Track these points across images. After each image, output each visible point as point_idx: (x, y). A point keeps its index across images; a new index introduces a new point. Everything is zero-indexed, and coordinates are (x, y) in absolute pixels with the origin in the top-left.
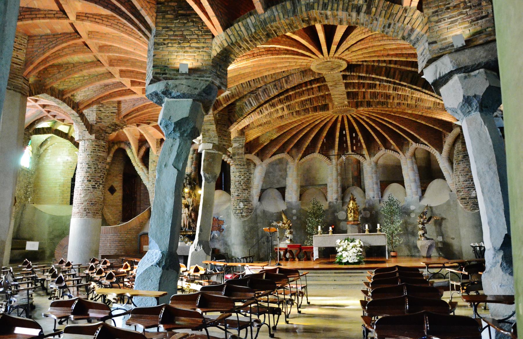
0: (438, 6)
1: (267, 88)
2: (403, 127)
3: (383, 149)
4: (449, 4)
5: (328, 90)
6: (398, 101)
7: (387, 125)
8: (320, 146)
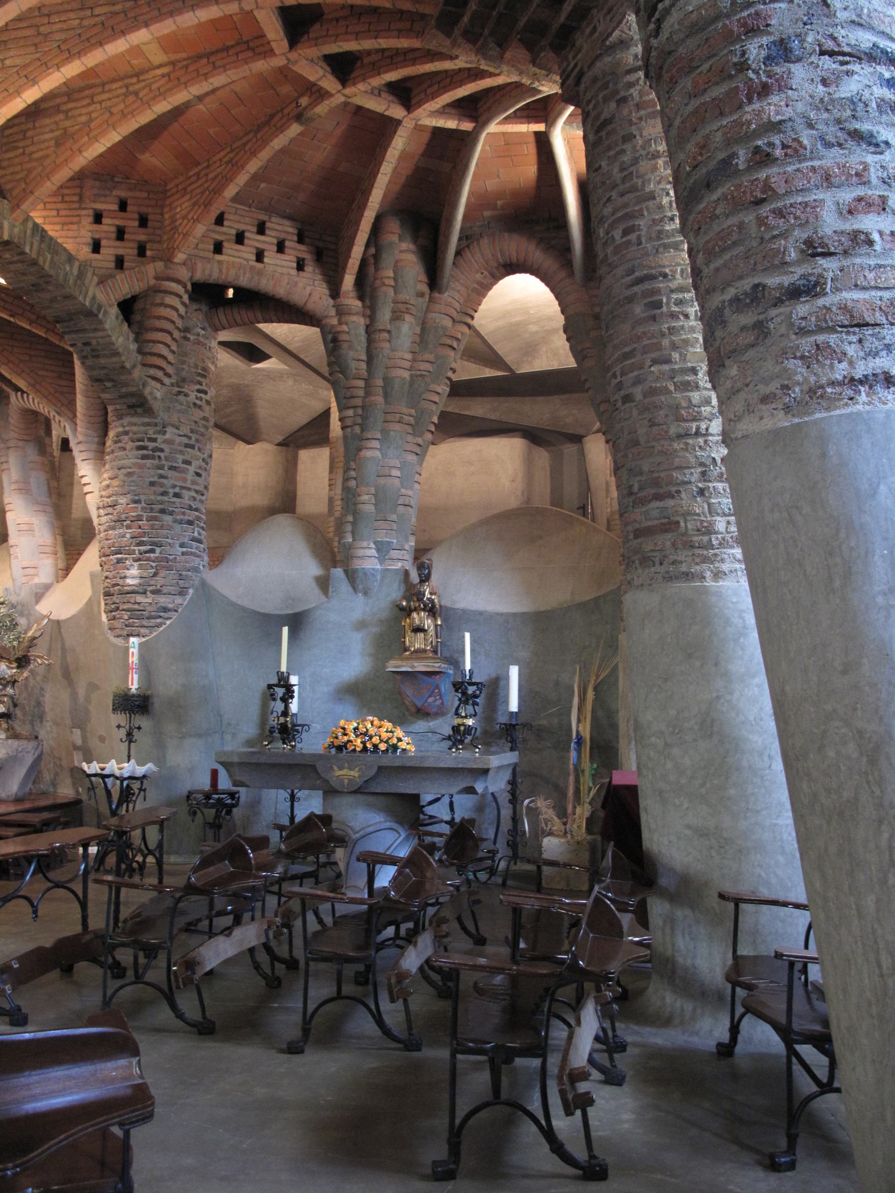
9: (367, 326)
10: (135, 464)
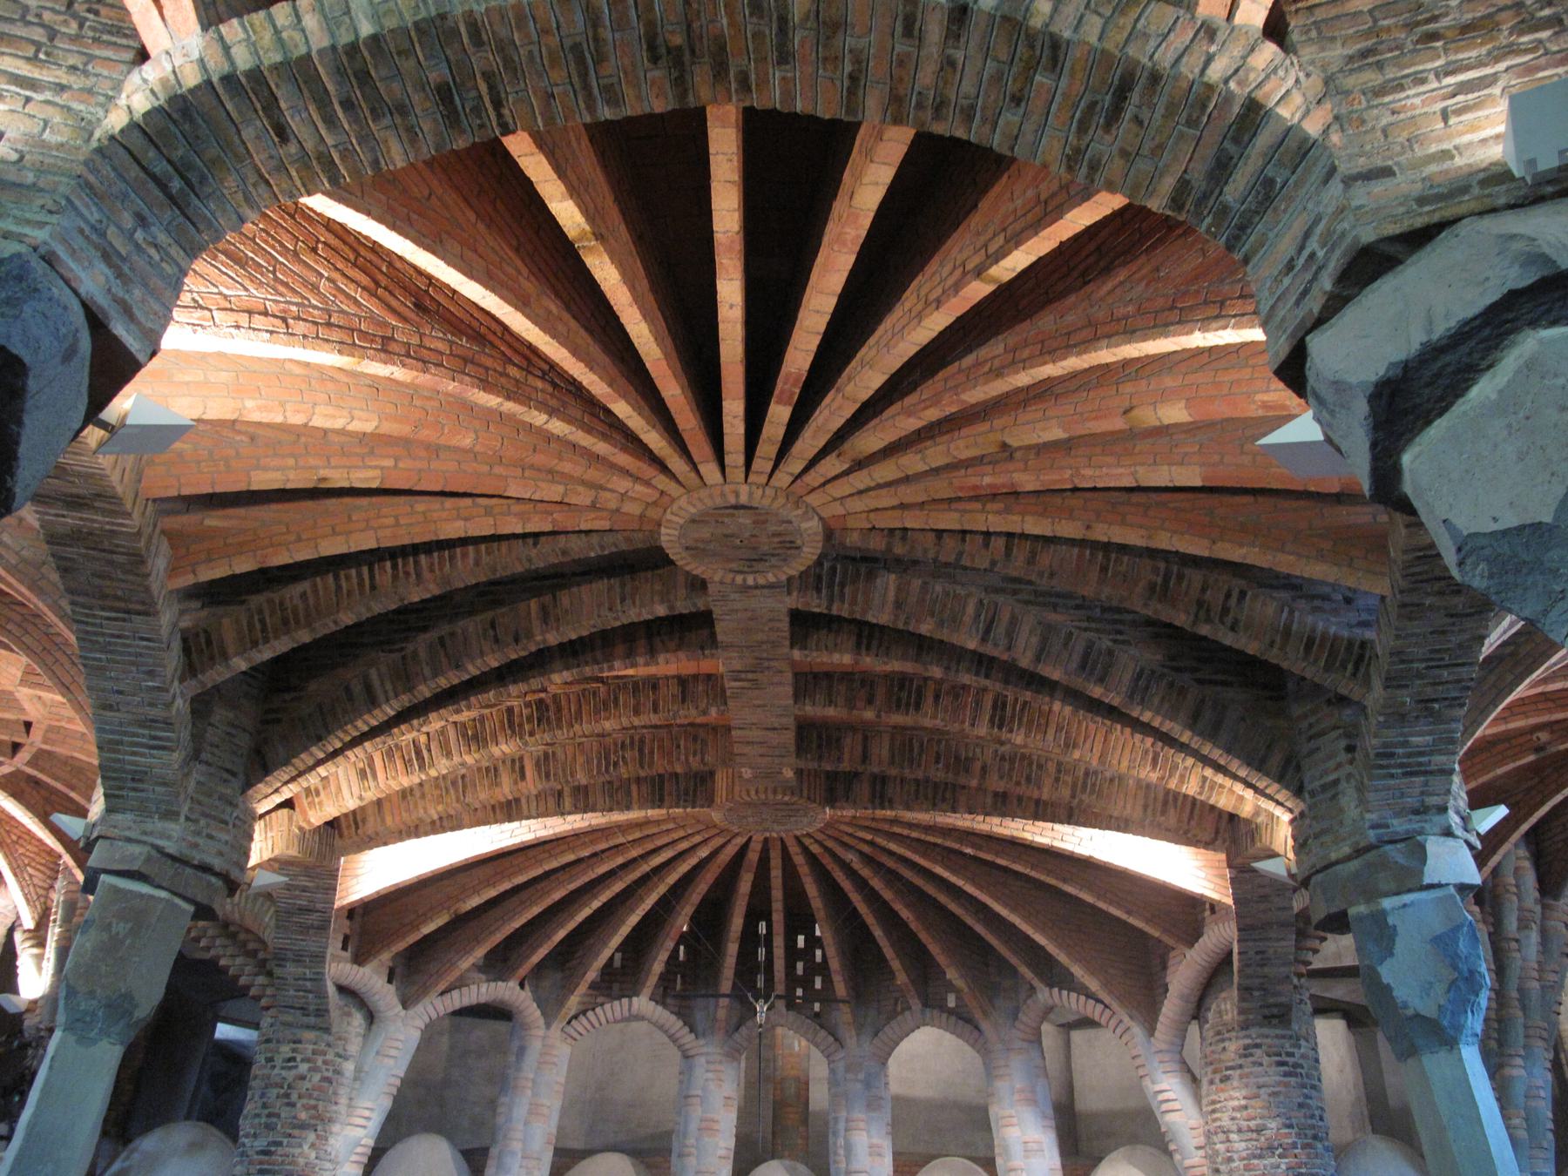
0: (1375, 31)
1: (452, 634)
2: (1004, 912)
3: (916, 1004)
4: (1434, 19)
5: (721, 696)
6: (1000, 786)
7: (943, 899)
8: (658, 967)
9: (1490, 934)
10: (1279, 1084)
